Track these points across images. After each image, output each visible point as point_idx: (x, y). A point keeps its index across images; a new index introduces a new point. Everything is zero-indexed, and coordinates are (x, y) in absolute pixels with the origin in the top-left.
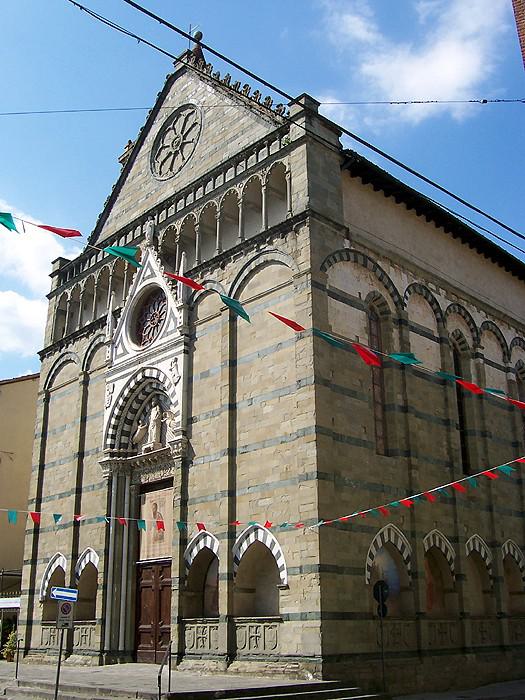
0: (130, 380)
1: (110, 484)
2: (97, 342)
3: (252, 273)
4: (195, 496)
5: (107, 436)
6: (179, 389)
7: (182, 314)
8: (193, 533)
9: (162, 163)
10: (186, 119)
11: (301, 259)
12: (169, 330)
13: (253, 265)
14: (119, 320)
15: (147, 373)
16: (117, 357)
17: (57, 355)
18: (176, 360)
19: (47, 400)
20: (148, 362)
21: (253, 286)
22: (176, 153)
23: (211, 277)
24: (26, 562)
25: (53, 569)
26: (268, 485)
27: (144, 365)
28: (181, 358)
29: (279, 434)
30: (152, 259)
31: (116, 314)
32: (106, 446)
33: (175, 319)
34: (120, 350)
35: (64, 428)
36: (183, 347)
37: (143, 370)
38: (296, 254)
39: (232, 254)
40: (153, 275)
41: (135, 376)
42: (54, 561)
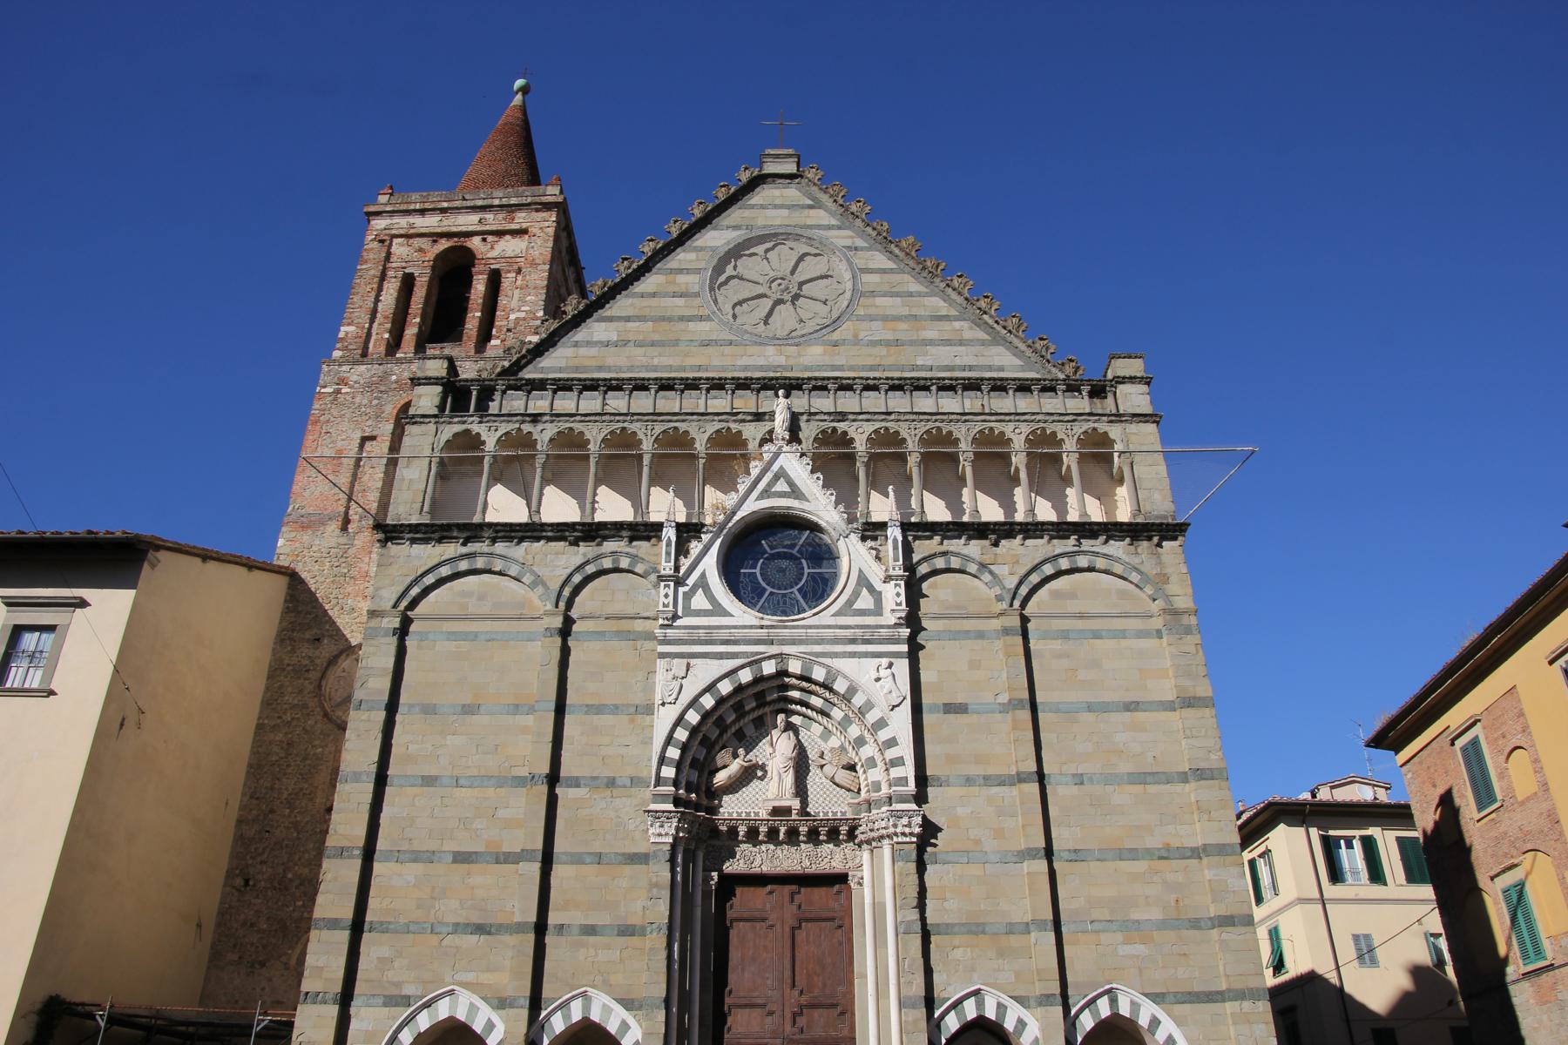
0: (742, 667)
1: (672, 860)
2: (607, 563)
3: (1059, 574)
4: (947, 919)
5: (662, 760)
6: (901, 723)
7: (902, 591)
8: (948, 987)
9: (740, 303)
10: (801, 259)
11: (1173, 588)
12: (859, 605)
13: (1064, 564)
14: (695, 547)
15: (795, 667)
16: (689, 612)
17: (451, 549)
18: (890, 666)
19: (403, 632)
20: (802, 648)
21: (1056, 595)
22: (779, 302)
23: (965, 551)
24: (315, 997)
25: (424, 1022)
26: (1137, 921)
27: (787, 649)
28: (902, 666)
29: (1154, 842)
30: (796, 466)
31: (689, 531)
32: (659, 781)
33: (877, 596)
34: (699, 601)
35: (469, 710)
36: (904, 648)
37: (780, 657)
38: (1164, 578)
39: (1020, 532)
40: (795, 492)
41: (759, 661)
42: (427, 1005)
